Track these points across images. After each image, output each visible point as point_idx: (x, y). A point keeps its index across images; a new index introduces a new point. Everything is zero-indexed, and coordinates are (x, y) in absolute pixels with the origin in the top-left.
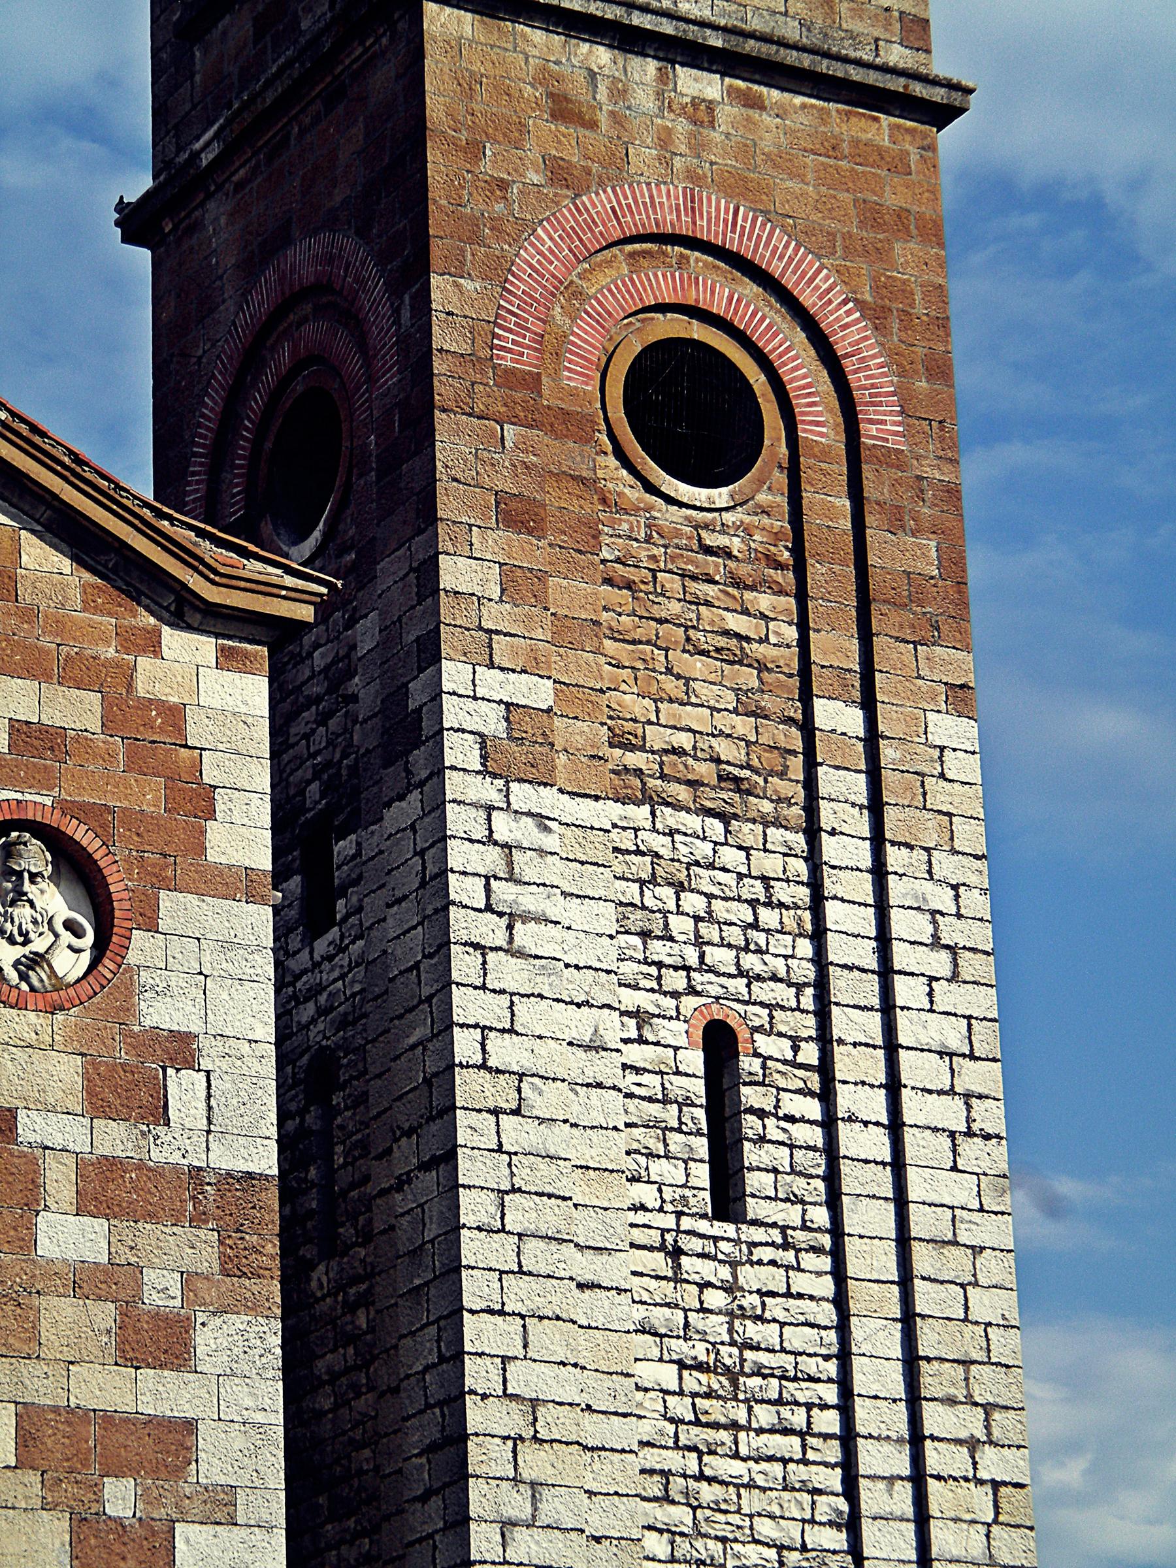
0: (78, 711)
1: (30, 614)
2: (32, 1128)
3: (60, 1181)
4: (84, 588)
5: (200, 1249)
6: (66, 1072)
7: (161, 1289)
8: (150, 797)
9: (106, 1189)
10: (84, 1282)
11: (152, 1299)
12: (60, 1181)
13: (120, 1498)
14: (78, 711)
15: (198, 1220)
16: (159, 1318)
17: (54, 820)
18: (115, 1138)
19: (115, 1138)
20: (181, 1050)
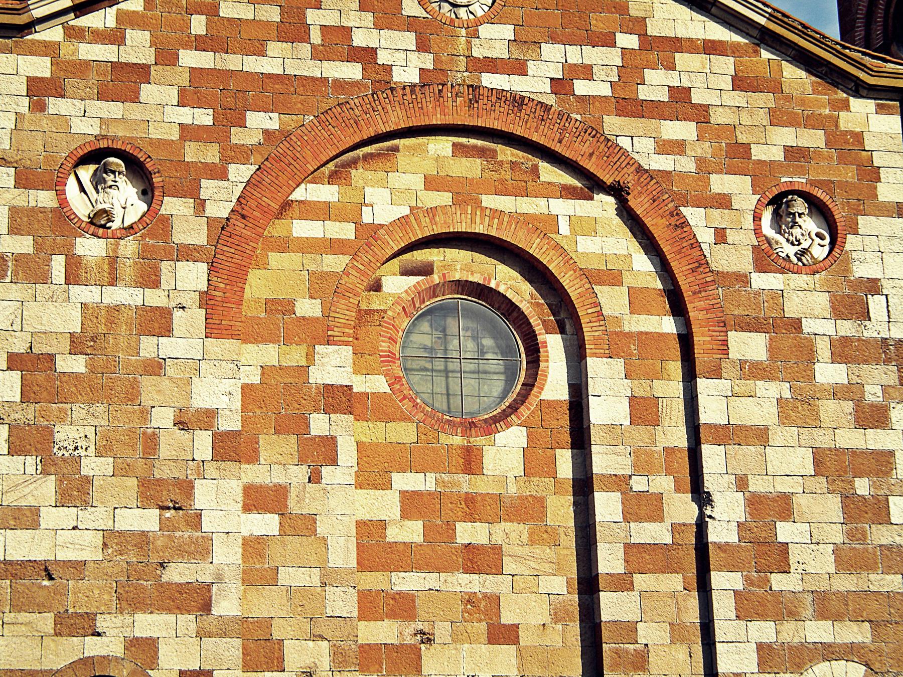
0: (814, 139)
1: (789, 98)
2: (808, 326)
3: (823, 349)
4: (813, 83)
5: (888, 374)
6: (822, 301)
7: (873, 393)
8: (849, 174)
9: (844, 351)
10: (837, 393)
11: (869, 398)
12: (823, 349)
13: (862, 487)
14: (814, 139)
15: (887, 361)
16: (872, 406)
17: (807, 189)
18: (847, 328)
19: (847, 328)
20: (873, 286)
